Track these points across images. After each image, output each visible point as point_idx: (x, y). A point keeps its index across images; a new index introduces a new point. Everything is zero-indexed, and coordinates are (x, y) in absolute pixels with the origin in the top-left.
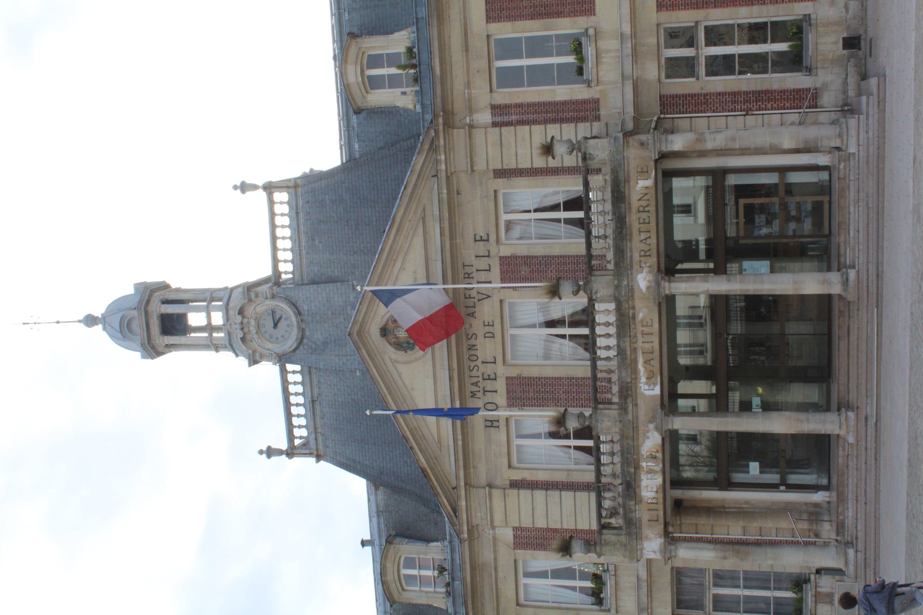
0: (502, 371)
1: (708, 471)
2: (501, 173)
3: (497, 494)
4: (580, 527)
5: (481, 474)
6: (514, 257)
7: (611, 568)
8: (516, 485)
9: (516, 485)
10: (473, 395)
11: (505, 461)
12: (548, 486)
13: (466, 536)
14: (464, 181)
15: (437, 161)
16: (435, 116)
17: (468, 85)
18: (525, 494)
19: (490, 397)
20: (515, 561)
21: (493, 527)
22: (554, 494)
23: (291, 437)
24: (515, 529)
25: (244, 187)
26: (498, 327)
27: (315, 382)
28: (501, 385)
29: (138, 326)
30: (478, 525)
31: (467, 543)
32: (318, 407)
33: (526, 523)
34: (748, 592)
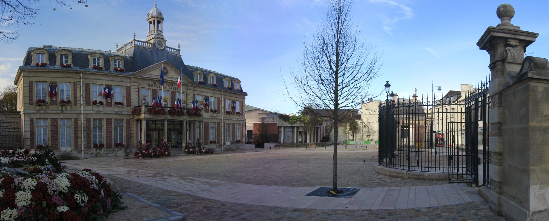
0: (158, 89)
1: (150, 127)
2: (187, 93)
3: (137, 84)
4: (131, 101)
5: (140, 82)
6: (175, 94)
7: (124, 106)
8: (139, 88)
9: (139, 88)
10: (154, 82)
11: (143, 87)
12: (139, 95)
13: (130, 76)
14: (186, 87)
15: (190, 84)
16: (196, 85)
17: (198, 91)
18: (137, 90)
19: (154, 86)
20: (123, 86)
21: (130, 82)
22: (138, 96)
23: (137, 41)
24: (130, 87)
25: (179, 45)
26: (165, 89)
27: (148, 49)
28: (156, 88)
29: (159, 16)
30: (130, 79)
31: (129, 76)
32: (144, 49)
33: (132, 90)
34: (119, 134)
